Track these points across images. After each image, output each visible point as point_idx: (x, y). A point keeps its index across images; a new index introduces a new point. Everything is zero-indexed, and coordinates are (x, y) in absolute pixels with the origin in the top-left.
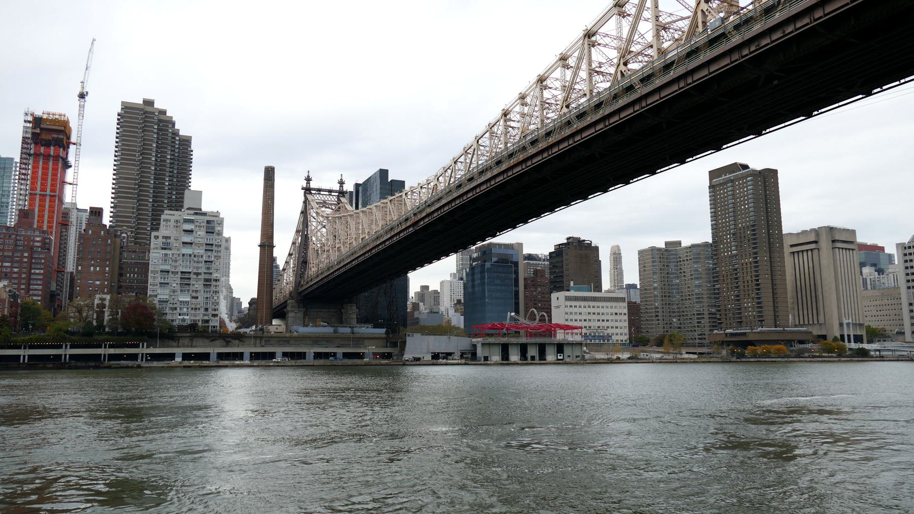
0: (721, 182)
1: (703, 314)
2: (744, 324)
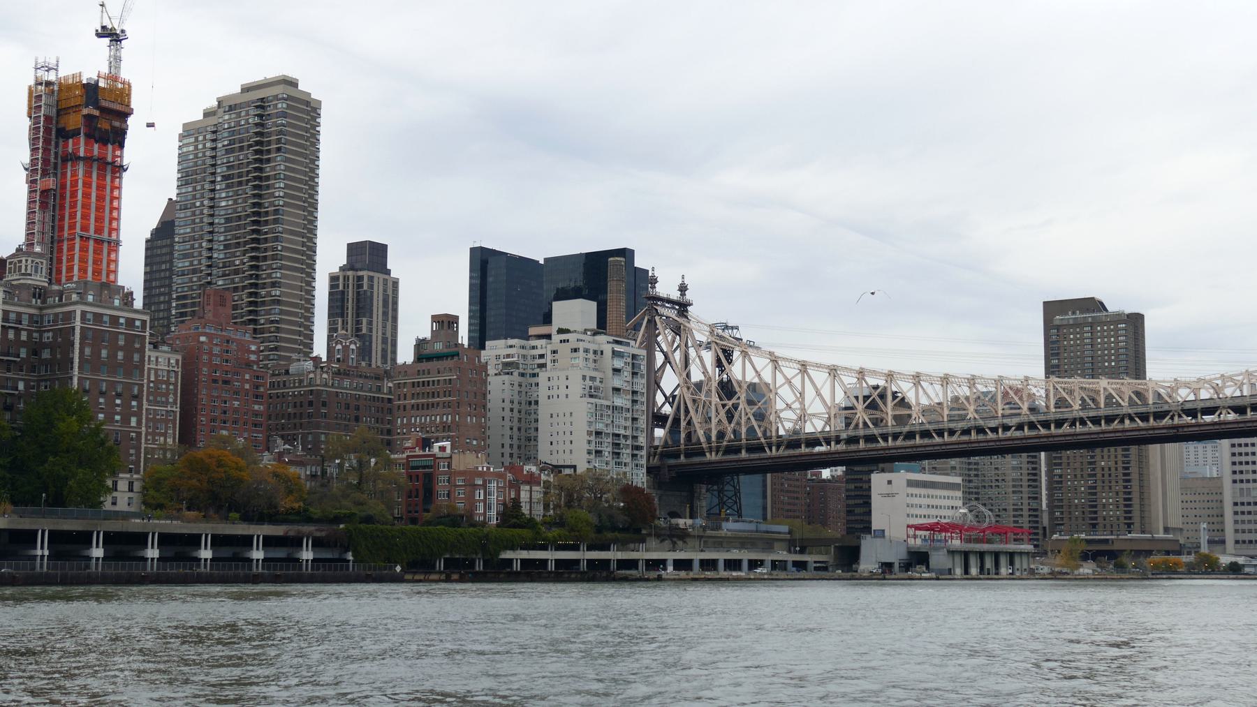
0: (1071, 322)
1: (1022, 510)
2: (1100, 527)
